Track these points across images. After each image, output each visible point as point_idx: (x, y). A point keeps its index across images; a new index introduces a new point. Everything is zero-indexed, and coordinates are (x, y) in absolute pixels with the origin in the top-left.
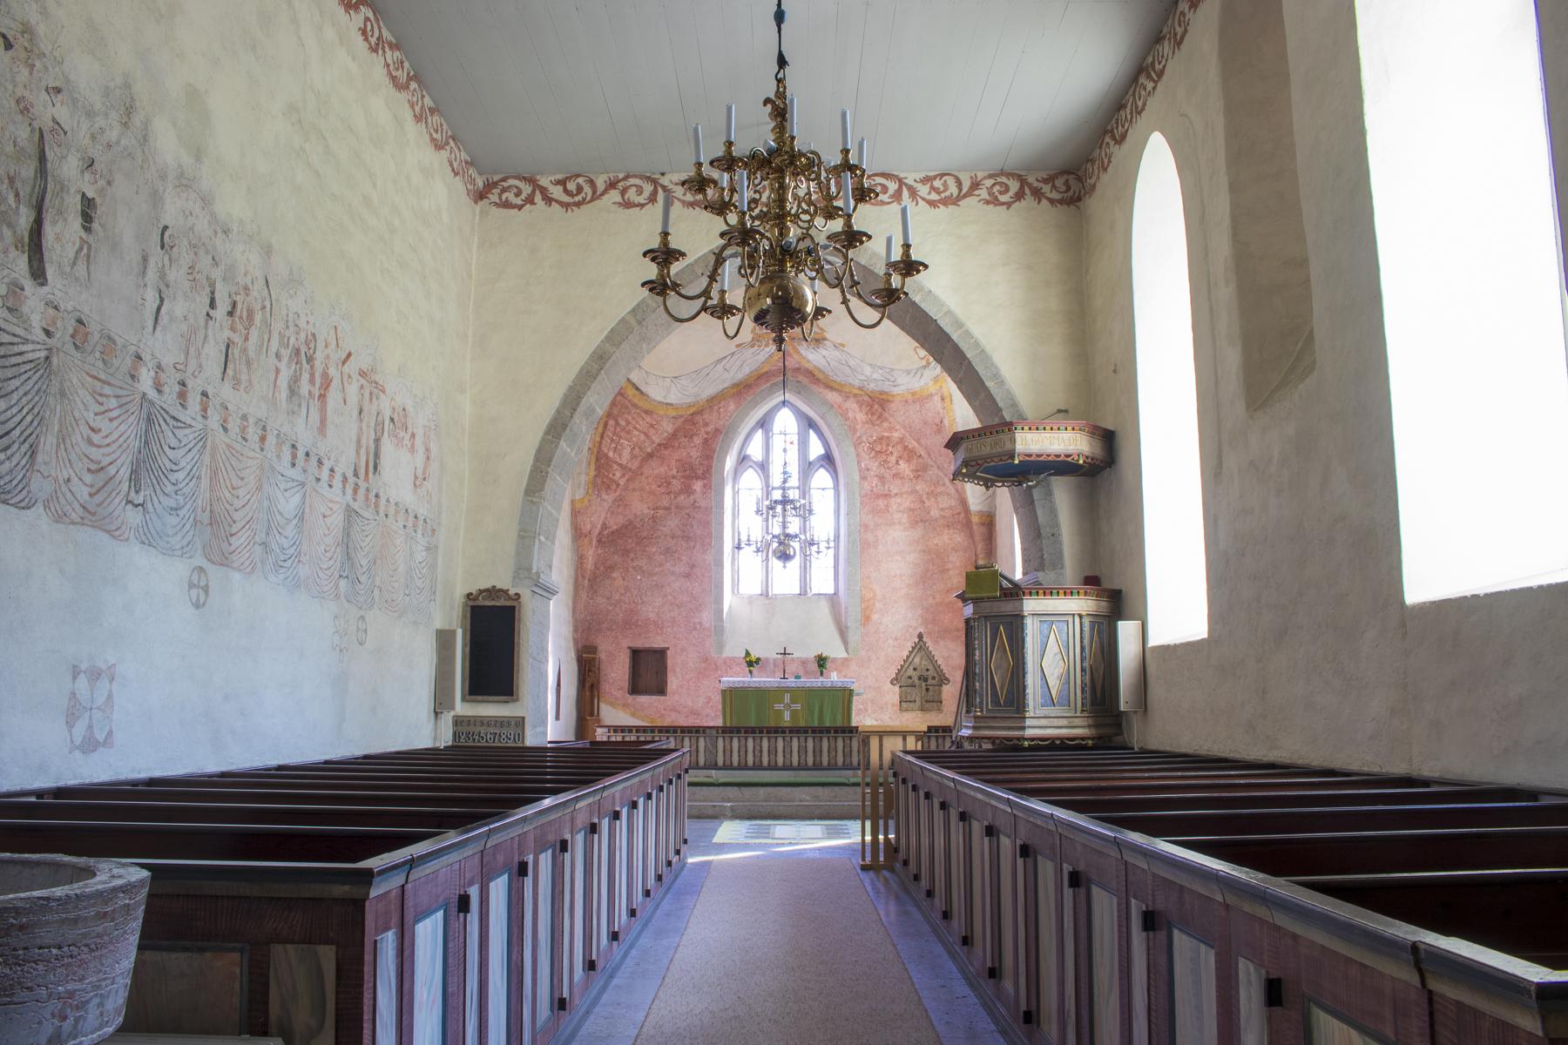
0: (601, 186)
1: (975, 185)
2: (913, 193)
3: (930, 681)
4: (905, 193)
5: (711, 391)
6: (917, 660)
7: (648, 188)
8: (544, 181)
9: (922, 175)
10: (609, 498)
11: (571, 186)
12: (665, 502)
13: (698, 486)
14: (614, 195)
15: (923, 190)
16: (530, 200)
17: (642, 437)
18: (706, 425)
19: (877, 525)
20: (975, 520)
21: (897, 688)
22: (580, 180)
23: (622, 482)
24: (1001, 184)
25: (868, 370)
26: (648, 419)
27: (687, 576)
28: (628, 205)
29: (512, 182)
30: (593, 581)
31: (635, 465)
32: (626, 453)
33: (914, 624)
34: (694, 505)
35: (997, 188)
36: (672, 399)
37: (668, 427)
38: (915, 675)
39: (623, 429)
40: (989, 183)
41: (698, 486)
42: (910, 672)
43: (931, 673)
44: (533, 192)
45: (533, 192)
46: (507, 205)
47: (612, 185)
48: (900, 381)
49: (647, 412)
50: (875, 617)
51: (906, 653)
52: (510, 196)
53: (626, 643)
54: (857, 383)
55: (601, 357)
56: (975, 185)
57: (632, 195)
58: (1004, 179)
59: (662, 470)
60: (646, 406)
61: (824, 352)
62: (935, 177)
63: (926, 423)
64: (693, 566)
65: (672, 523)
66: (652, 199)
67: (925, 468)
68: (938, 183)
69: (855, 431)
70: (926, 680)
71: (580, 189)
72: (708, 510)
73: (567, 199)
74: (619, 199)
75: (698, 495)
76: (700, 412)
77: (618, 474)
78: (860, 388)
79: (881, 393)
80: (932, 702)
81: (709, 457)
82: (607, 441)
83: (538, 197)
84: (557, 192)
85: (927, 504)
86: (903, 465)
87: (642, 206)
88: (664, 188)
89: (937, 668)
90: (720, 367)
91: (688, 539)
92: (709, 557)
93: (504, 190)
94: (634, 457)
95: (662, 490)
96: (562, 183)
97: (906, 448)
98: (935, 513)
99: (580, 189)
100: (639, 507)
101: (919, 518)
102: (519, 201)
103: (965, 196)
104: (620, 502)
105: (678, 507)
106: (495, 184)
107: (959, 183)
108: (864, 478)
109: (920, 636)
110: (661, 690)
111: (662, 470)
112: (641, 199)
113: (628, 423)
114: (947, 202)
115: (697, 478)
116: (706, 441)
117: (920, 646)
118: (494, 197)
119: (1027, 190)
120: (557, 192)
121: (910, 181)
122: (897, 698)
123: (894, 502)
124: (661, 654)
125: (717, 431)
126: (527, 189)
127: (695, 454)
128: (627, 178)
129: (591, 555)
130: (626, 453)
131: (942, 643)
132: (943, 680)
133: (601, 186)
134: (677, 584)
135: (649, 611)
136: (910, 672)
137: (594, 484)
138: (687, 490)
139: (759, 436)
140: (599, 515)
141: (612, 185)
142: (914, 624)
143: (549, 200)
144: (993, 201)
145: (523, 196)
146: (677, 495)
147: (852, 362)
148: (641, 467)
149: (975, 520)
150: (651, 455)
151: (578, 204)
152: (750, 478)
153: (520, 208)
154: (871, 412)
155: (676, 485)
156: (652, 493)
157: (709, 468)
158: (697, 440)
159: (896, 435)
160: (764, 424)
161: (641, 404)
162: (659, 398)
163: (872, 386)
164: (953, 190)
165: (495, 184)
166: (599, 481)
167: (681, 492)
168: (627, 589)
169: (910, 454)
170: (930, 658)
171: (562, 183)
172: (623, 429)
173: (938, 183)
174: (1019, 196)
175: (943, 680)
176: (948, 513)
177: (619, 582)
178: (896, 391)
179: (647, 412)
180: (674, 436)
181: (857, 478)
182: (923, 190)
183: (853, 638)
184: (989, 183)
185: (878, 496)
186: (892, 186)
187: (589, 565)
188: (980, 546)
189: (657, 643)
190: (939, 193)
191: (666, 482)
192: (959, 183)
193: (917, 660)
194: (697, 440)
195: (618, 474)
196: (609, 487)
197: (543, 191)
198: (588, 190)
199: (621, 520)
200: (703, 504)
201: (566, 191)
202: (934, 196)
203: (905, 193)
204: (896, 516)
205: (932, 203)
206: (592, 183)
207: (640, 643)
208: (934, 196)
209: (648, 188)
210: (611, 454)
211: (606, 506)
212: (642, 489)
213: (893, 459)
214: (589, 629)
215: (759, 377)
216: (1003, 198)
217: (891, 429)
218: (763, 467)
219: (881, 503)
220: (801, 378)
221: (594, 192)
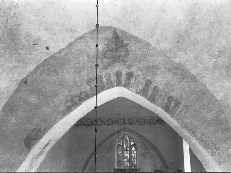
2: (147, 123)
4: (146, 123)
11: (88, 122)
15: (149, 122)
44: (81, 123)
45: (81, 123)
66: (102, 124)
71: (89, 122)
83: (82, 124)
107: (155, 120)
112: (100, 124)
114: (152, 124)
143: (84, 124)
164: (154, 121)
173: (151, 121)
190: (151, 122)
192: (155, 120)
203: (146, 123)
208: (151, 123)
209: (101, 122)
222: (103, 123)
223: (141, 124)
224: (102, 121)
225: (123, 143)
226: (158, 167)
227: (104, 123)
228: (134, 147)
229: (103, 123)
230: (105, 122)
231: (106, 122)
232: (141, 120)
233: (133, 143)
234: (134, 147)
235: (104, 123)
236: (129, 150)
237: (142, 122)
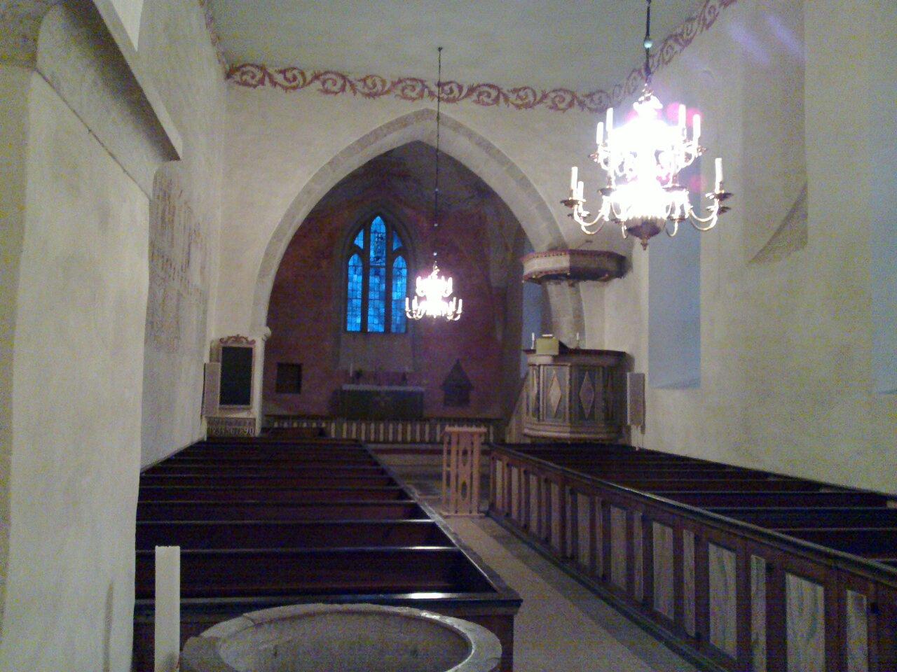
0: (309, 78)
1: (545, 96)
2: (506, 99)
7: (340, 82)
8: (271, 71)
9: (512, 88)
11: (289, 75)
13: (324, 263)
14: (318, 84)
15: (512, 97)
16: (262, 82)
22: (295, 72)
24: (561, 96)
28: (327, 92)
29: (249, 68)
35: (557, 99)
40: (553, 95)
41: (324, 263)
46: (246, 84)
47: (316, 77)
52: (247, 78)
55: (309, 192)
56: (545, 96)
57: (329, 85)
58: (561, 93)
62: (520, 90)
66: (343, 89)
68: (521, 93)
73: (286, 84)
74: (321, 87)
84: (279, 78)
87: (336, 93)
88: (350, 82)
93: (243, 73)
96: (283, 72)
99: (295, 78)
102: (254, 82)
103: (538, 103)
106: (238, 69)
107: (535, 95)
109: (458, 361)
110: (298, 388)
112: (335, 89)
114: (528, 106)
117: (458, 367)
118: (237, 77)
119: (575, 102)
120: (279, 78)
121: (505, 91)
124: (299, 367)
126: (259, 75)
128: (326, 73)
133: (309, 78)
139: (361, 234)
141: (316, 77)
143: (274, 84)
144: (554, 107)
145: (257, 79)
151: (294, 88)
152: (354, 260)
153: (255, 86)
160: (366, 226)
164: (531, 98)
165: (238, 69)
171: (283, 72)
173: (521, 93)
174: (571, 105)
182: (512, 97)
184: (553, 95)
186: (494, 93)
189: (296, 360)
190: (522, 100)
192: (535, 95)
197: (270, 76)
198: (300, 78)
201: (286, 78)
202: (519, 102)
205: (518, 106)
206: (302, 74)
208: (519, 102)
209: (340, 82)
216: (562, 106)
218: (364, 254)
221: (305, 80)
222: (348, 84)
223: (488, 104)
224: (344, 78)
227: (352, 85)
229: (348, 84)
230: (354, 82)
231: (360, 85)
232: (486, 89)
235: (352, 85)
237: (489, 96)
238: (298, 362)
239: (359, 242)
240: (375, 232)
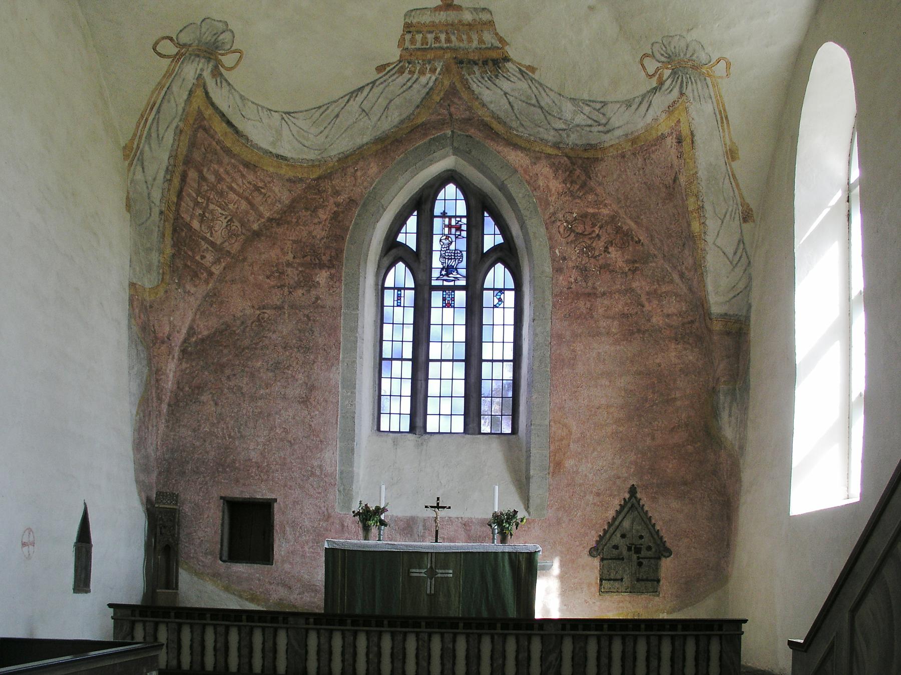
3: (644, 553)
5: (343, 145)
6: (626, 524)
10: (199, 291)
12: (276, 298)
13: (322, 277)
17: (244, 205)
18: (337, 193)
19: (575, 335)
20: (717, 326)
21: (596, 562)
23: (216, 270)
25: (568, 109)
26: (251, 177)
27: (305, 401)
30: (175, 406)
31: (235, 247)
32: (220, 225)
33: (624, 473)
34: (316, 304)
36: (286, 149)
37: (282, 195)
38: (622, 543)
39: (213, 188)
42: (617, 539)
43: (647, 541)
48: (615, 122)
49: (247, 165)
50: (569, 463)
51: (611, 513)
53: (217, 492)
54: (551, 136)
59: (274, 254)
60: (247, 155)
61: (506, 85)
63: (650, 187)
64: (312, 388)
65: (286, 328)
67: (645, 258)
69: (548, 204)
70: (638, 550)
72: (336, 310)
75: (322, 291)
76: (328, 176)
77: (210, 258)
78: (556, 146)
79: (589, 147)
80: (646, 581)
81: (340, 238)
82: (187, 203)
85: (648, 307)
86: (614, 254)
89: (656, 535)
90: (354, 105)
91: (307, 350)
92: (336, 376)
94: (232, 234)
95: (272, 282)
97: (618, 230)
98: (657, 320)
100: (240, 305)
101: (633, 328)
104: (213, 297)
105: (292, 306)
108: (558, 270)
109: (633, 491)
111: (274, 254)
113: (220, 179)
115: (322, 266)
116: (336, 215)
117: (631, 504)
122: (597, 574)
123: (601, 305)
125: (352, 202)
127: (319, 232)
129: (171, 369)
130: (220, 225)
131: (661, 500)
132: (663, 551)
134: (291, 412)
135: (251, 449)
136: (617, 539)
137: (173, 269)
138: (308, 283)
140: (183, 317)
142: (624, 473)
146: (292, 289)
147: (545, 101)
148: (243, 250)
149: (717, 326)
150: (257, 234)
154: (570, 179)
155: (292, 275)
156: (259, 286)
157: (339, 251)
158: (323, 215)
159: (605, 211)
161: (236, 149)
162: (265, 145)
163: (573, 138)
166: (179, 263)
167: (298, 285)
168: (221, 418)
169: (624, 238)
170: (646, 521)
172: (213, 188)
175: (663, 551)
176: (675, 321)
177: (210, 408)
178: (609, 140)
179: (247, 165)
180: (291, 208)
181: (548, 269)
183: (537, 491)
185: (577, 296)
187: (169, 384)
188: (721, 367)
189: (262, 493)
191: (277, 271)
193: (626, 524)
194: (323, 215)
195: (210, 258)
196: (195, 275)
199: (214, 323)
200: (329, 303)
204: (603, 323)
207: (237, 492)
210: (196, 224)
211: (194, 302)
212: (244, 281)
213: (600, 245)
214: (168, 471)
215: (414, 130)
217: (597, 204)
219: (582, 305)
220: (472, 131)
225: (425, 233)
226: (678, 395)
228: (500, 267)
233: (500, 240)
234: (500, 267)
236: (463, 282)
238: (269, 496)
239: (409, 236)
240: (444, 215)
